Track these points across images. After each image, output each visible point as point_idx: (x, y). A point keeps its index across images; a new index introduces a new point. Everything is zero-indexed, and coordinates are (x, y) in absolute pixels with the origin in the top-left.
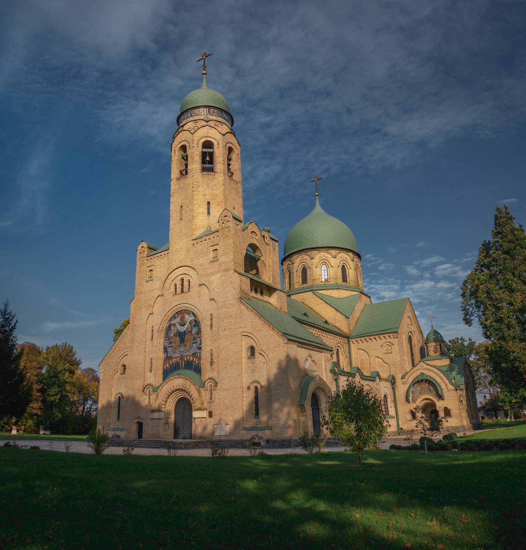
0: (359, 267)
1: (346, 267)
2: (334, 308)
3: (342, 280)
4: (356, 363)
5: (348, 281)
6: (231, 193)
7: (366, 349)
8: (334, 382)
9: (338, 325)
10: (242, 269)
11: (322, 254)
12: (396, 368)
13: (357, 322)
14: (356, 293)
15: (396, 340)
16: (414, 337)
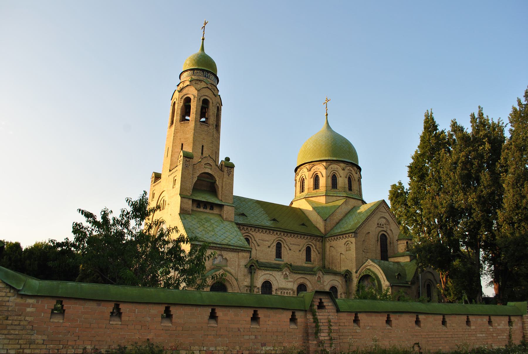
0: (352, 174)
1: (336, 176)
2: (317, 212)
3: (330, 188)
4: (328, 258)
5: (338, 188)
6: (201, 135)
7: (335, 247)
8: (250, 276)
9: (318, 226)
10: (189, 193)
11: (315, 167)
12: (352, 264)
13: (338, 223)
14: (343, 198)
15: (354, 239)
16: (389, 235)
